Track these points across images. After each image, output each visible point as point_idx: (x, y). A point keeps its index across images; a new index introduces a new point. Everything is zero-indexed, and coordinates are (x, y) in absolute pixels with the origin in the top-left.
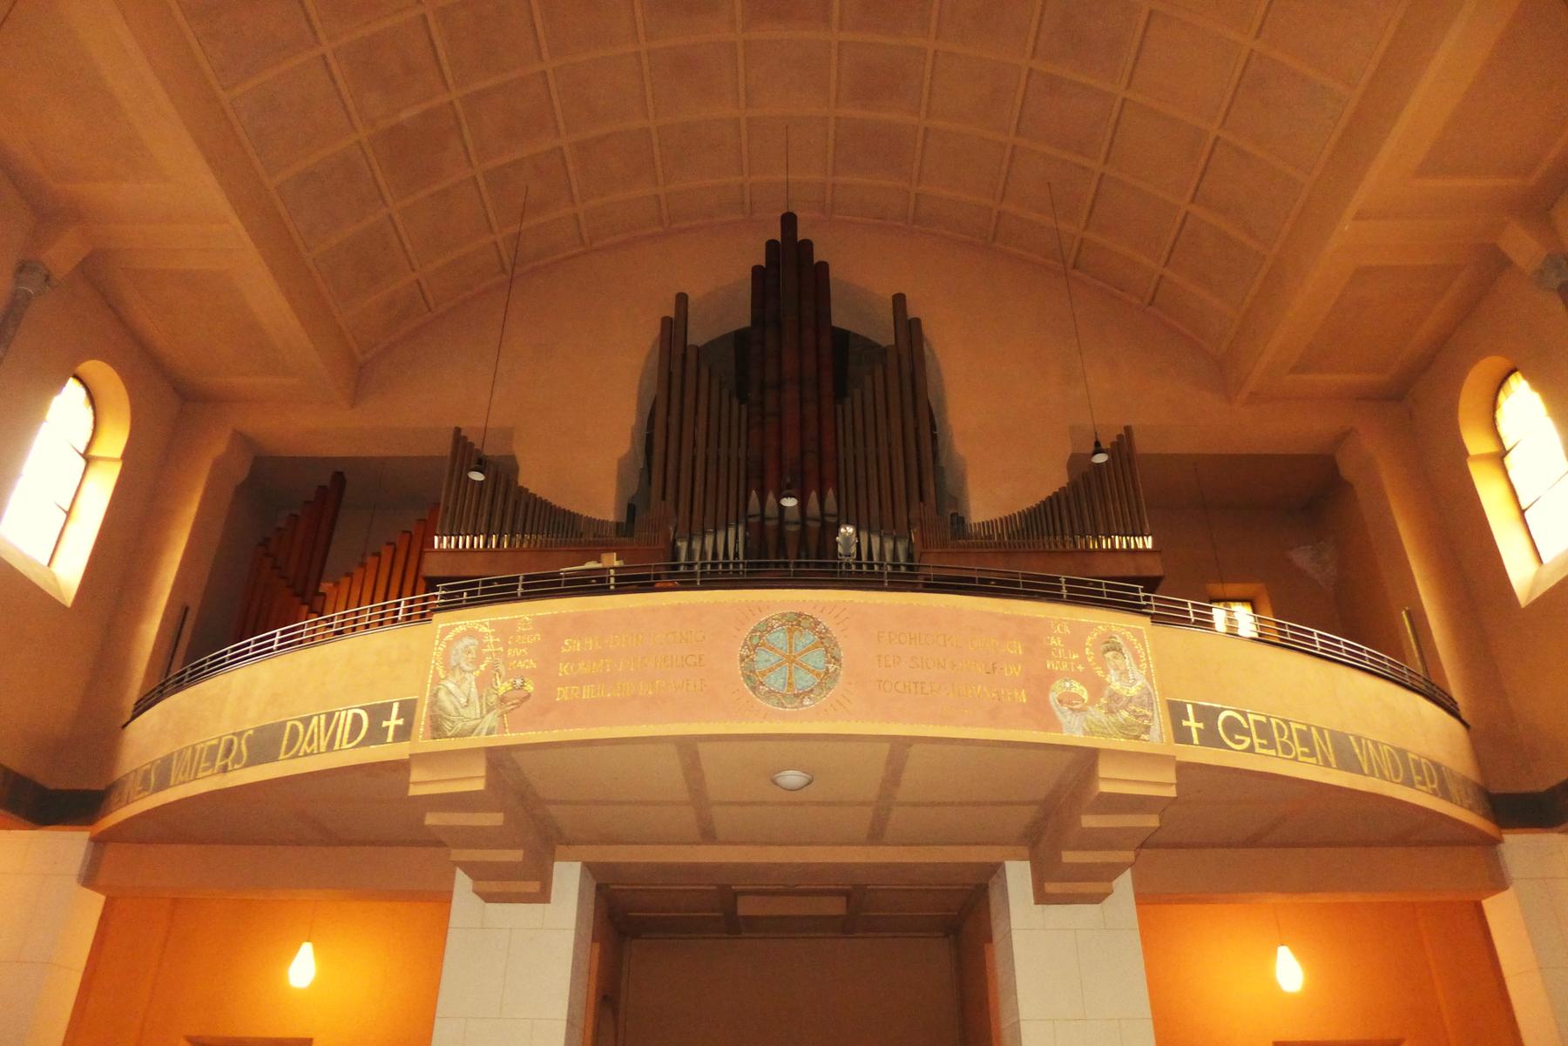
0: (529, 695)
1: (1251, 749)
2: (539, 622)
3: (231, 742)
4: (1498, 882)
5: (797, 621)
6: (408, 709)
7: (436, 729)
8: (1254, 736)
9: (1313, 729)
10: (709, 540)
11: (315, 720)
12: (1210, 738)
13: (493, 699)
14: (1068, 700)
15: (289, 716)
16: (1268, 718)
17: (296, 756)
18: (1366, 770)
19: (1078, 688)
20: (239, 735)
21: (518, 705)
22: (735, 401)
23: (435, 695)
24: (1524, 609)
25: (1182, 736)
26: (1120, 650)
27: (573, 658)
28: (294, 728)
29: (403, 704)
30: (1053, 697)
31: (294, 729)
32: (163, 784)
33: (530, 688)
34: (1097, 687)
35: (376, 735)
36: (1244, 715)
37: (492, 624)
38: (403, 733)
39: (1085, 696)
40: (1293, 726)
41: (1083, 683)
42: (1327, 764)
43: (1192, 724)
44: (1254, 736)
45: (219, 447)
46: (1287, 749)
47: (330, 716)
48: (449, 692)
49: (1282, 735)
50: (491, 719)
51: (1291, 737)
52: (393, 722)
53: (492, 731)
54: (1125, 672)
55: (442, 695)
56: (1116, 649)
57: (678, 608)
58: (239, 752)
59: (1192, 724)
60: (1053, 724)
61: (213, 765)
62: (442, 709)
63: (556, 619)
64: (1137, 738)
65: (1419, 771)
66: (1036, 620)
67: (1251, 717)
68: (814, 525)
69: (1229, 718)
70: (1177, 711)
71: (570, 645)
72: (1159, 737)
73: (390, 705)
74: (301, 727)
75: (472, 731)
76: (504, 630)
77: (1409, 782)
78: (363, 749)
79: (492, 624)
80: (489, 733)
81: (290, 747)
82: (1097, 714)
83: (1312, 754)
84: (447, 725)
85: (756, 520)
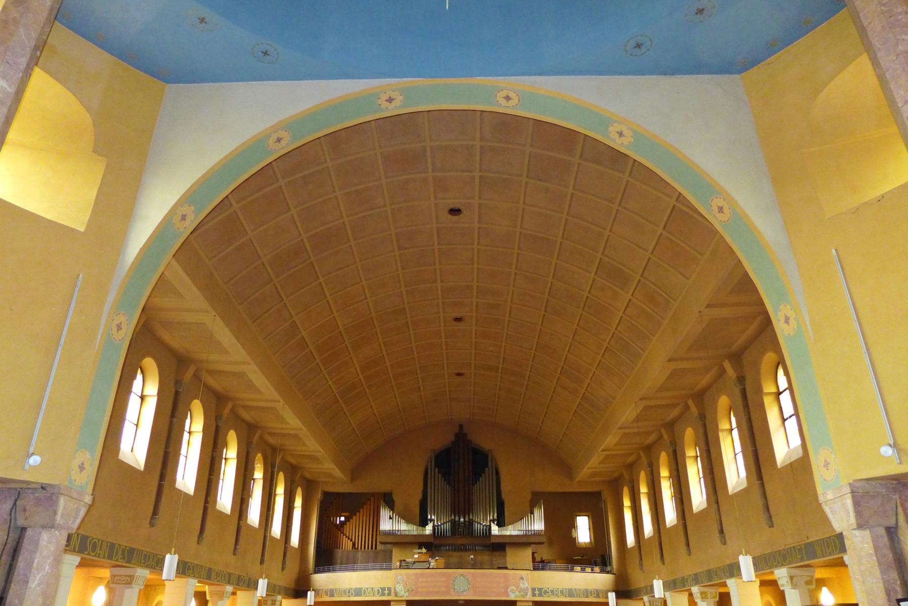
0: (413, 590)
6: (389, 589)
7: (396, 595)
8: (550, 594)
9: (564, 590)
10: (442, 526)
14: (511, 591)
15: (364, 585)
18: (575, 596)
19: (515, 588)
20: (352, 589)
21: (411, 592)
25: (534, 595)
27: (421, 582)
28: (364, 590)
30: (509, 590)
31: (364, 590)
32: (332, 595)
33: (414, 588)
34: (518, 587)
35: (383, 594)
36: (548, 589)
37: (405, 574)
38: (389, 594)
41: (515, 587)
42: (566, 597)
44: (550, 594)
45: (319, 496)
46: (557, 595)
47: (372, 588)
51: (558, 592)
52: (386, 592)
54: (524, 584)
55: (396, 588)
56: (522, 578)
57: (441, 573)
59: (537, 592)
60: (508, 595)
61: (346, 594)
65: (591, 593)
66: (508, 574)
70: (533, 590)
71: (421, 579)
72: (529, 597)
75: (403, 596)
76: (407, 575)
77: (587, 597)
78: (381, 597)
82: (517, 593)
85: (453, 521)
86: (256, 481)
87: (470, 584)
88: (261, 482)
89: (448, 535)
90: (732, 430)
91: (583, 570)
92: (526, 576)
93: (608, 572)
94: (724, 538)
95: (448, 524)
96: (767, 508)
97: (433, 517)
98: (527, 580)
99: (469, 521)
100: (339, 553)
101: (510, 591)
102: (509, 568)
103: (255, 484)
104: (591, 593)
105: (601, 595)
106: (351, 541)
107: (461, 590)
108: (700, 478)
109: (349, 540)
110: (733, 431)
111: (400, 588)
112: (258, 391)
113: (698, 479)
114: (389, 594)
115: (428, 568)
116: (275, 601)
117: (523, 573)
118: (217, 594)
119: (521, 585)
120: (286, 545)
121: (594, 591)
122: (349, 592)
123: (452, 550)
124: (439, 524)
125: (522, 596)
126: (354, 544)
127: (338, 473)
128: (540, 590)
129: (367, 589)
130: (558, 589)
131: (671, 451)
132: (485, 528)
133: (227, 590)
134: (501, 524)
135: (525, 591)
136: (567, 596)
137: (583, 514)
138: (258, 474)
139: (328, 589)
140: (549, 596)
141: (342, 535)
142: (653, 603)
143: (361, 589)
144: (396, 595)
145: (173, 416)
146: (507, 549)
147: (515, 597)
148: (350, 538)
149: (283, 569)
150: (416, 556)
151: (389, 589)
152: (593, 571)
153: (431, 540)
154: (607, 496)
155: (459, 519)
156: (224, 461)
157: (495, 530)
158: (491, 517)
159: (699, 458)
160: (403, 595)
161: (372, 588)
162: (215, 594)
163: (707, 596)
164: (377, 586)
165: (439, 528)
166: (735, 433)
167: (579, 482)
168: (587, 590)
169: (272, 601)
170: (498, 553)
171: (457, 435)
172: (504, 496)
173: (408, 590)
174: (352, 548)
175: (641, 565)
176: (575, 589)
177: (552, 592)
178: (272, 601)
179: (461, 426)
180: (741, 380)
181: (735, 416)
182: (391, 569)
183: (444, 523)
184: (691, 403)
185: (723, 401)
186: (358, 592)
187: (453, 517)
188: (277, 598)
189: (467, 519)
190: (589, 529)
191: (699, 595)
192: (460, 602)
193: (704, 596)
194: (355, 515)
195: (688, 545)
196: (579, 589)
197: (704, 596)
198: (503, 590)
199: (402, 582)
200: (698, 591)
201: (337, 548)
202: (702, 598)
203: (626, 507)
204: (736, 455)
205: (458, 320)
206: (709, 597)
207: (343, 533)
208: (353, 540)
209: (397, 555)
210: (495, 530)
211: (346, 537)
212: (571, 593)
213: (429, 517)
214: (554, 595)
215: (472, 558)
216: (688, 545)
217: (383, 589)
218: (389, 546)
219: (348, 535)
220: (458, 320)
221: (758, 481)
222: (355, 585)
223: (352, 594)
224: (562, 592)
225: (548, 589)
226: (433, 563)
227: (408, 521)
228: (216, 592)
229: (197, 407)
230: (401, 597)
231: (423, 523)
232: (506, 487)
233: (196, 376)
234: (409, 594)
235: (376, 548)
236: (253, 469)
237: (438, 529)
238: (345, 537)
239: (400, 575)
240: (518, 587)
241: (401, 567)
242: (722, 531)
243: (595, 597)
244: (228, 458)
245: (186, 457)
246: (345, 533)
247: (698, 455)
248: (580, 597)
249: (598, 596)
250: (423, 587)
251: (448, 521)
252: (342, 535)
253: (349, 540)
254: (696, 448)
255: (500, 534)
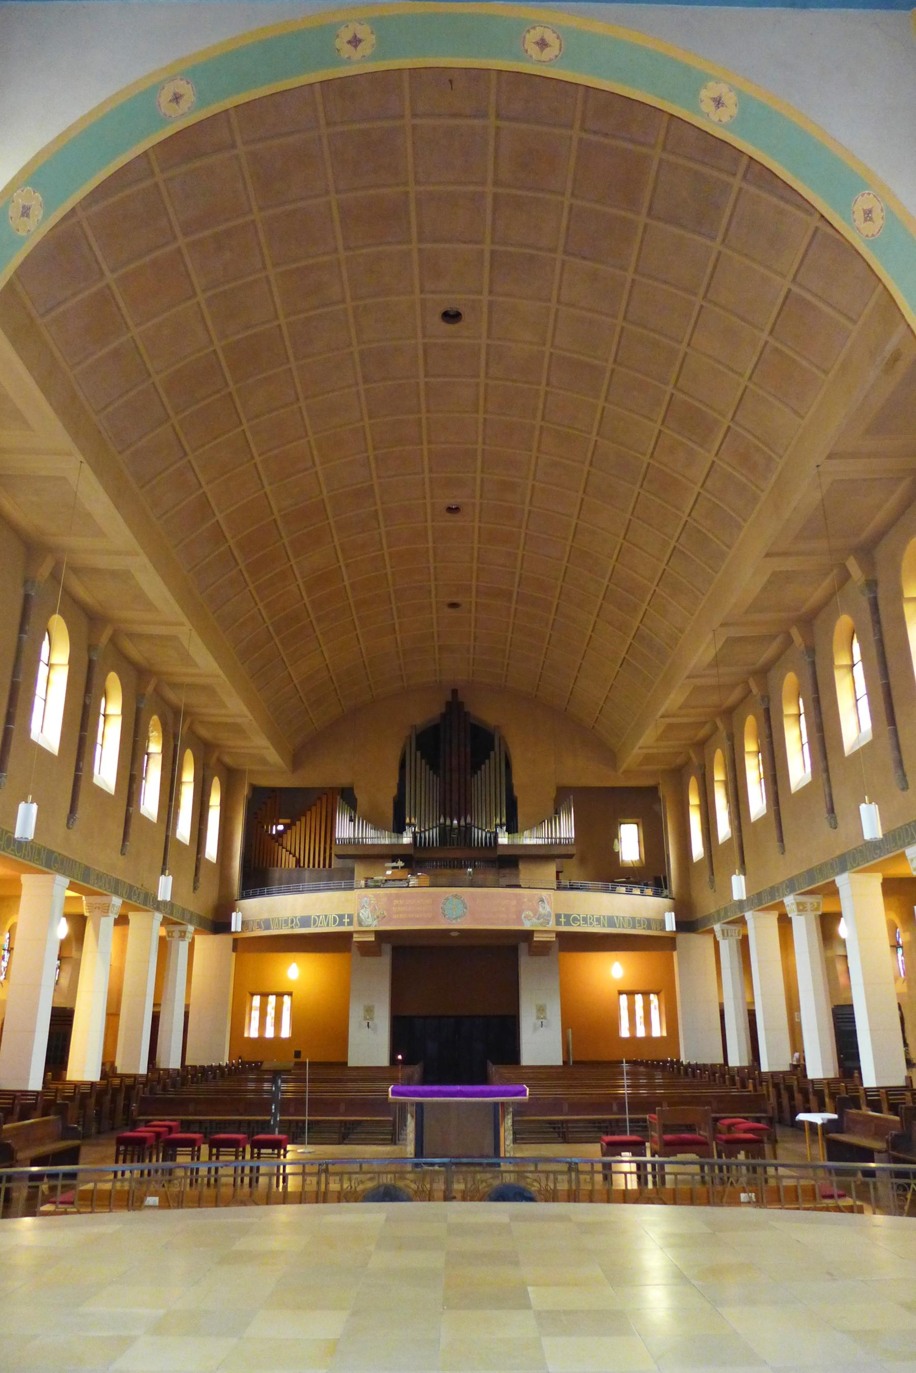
0: (385, 916)
1: (579, 925)
2: (386, 895)
3: (293, 919)
4: (675, 950)
5: (456, 896)
7: (360, 924)
8: (581, 922)
9: (602, 917)
10: (427, 833)
11: (321, 917)
12: (568, 923)
13: (375, 917)
15: (313, 913)
16: (587, 915)
17: (317, 927)
19: (530, 913)
20: (296, 917)
22: (435, 776)
23: (358, 914)
24: (846, 758)
25: (558, 923)
26: (543, 901)
27: (397, 906)
28: (314, 918)
29: (348, 915)
30: (523, 916)
31: (315, 919)
32: (268, 927)
34: (535, 912)
35: (341, 923)
36: (579, 915)
37: (373, 894)
39: (532, 915)
40: (595, 917)
42: (604, 926)
43: (563, 920)
44: (581, 922)
45: (245, 791)
46: (591, 924)
47: (326, 916)
48: (362, 914)
49: (590, 920)
50: (375, 922)
51: (593, 920)
52: (346, 920)
53: (375, 926)
54: (544, 908)
55: (361, 914)
56: (542, 901)
58: (296, 923)
59: (563, 920)
60: (523, 924)
61: (288, 925)
62: (362, 919)
63: (391, 894)
64: (545, 926)
66: (520, 894)
67: (581, 916)
68: (463, 829)
69: (574, 917)
70: (558, 916)
71: (396, 902)
72: (552, 926)
73: (345, 915)
74: (317, 918)
75: (370, 926)
76: (376, 896)
77: (634, 927)
79: (373, 894)
80: (375, 926)
81: (314, 924)
82: (534, 920)
83: (600, 924)
84: (363, 923)
86: (151, 756)
87: (466, 908)
88: (160, 758)
89: (435, 845)
90: (854, 665)
91: (629, 892)
92: (548, 897)
93: (666, 897)
94: (835, 819)
95: (435, 830)
96: (900, 764)
97: (413, 820)
98: (548, 902)
99: (466, 826)
100: (276, 873)
101: (525, 917)
102: (522, 886)
103: (151, 761)
104: (639, 922)
105: (653, 925)
106: (294, 856)
107: (454, 917)
108: (803, 745)
109: (291, 856)
110: (855, 668)
111: (365, 914)
112: (150, 606)
113: (800, 746)
114: (350, 923)
115: (408, 887)
116: (185, 932)
117: (544, 893)
118: (99, 908)
119: (541, 909)
120: (199, 856)
121: (644, 921)
122: (292, 921)
123: (440, 867)
124: (423, 830)
125: (541, 924)
126: (298, 862)
127: (273, 756)
128: (567, 916)
129: (319, 917)
130: (593, 916)
131: (761, 711)
132: (488, 835)
133: (113, 903)
134: (512, 829)
135: (546, 919)
136: (606, 925)
137: (630, 820)
138: (155, 747)
139: (261, 920)
140: (579, 925)
141: (280, 847)
142: (727, 933)
143: (310, 917)
144: (360, 924)
145: (22, 629)
146: (521, 866)
147: (532, 926)
148: (293, 851)
149: (195, 888)
150: (389, 872)
151: (350, 917)
152: (642, 893)
153: (411, 851)
154: (665, 792)
155: (452, 822)
156: (102, 718)
157: (504, 839)
158: (498, 821)
159: (803, 718)
160: (370, 923)
161: (326, 916)
162: (95, 908)
163: (804, 907)
164: (333, 913)
165: (423, 835)
166: (859, 670)
167: (625, 772)
168: (633, 919)
169: (180, 932)
170: (507, 871)
171: (449, 704)
172: (517, 792)
173: (378, 917)
174: (296, 866)
175: (712, 882)
176: (617, 917)
177: (585, 919)
178: (180, 932)
179: (455, 692)
180: (872, 585)
181: (859, 641)
182: (352, 889)
183: (425, 830)
184: (795, 633)
185: (844, 622)
186: (305, 921)
187: (442, 820)
188: (187, 928)
189: (463, 823)
190: (639, 842)
191: (794, 907)
192: (453, 934)
193: (801, 908)
194: (300, 820)
195: (781, 839)
196: (623, 917)
197: (801, 908)
198: (515, 917)
199: (370, 904)
200: (793, 901)
201: (273, 866)
202: (799, 910)
203: (692, 805)
204: (857, 700)
205: (453, 510)
206: (809, 910)
207: (282, 845)
208: (297, 854)
209: (360, 872)
210: (504, 839)
211: (287, 851)
212: (611, 922)
213: (407, 820)
214: (586, 923)
215: (470, 873)
216: (781, 839)
217: (341, 917)
218: (349, 863)
219: (289, 848)
220: (453, 510)
221: (889, 726)
222: (299, 913)
223: (296, 925)
224: (598, 920)
225: (579, 915)
226: (413, 881)
227: (377, 826)
228: (97, 905)
229: (58, 624)
230: (367, 926)
231: (399, 828)
232: (520, 777)
233: (55, 576)
234: (378, 922)
235: (330, 866)
236: (147, 738)
237: (421, 837)
238: (284, 850)
239: (366, 896)
240: (535, 912)
241: (367, 886)
242: (831, 810)
243: (644, 928)
244: (108, 715)
245: (45, 701)
246: (284, 845)
247: (802, 711)
248: (623, 927)
249: (649, 928)
250: (398, 913)
251: (435, 825)
252: (280, 847)
253: (291, 856)
254: (798, 700)
255: (510, 843)
